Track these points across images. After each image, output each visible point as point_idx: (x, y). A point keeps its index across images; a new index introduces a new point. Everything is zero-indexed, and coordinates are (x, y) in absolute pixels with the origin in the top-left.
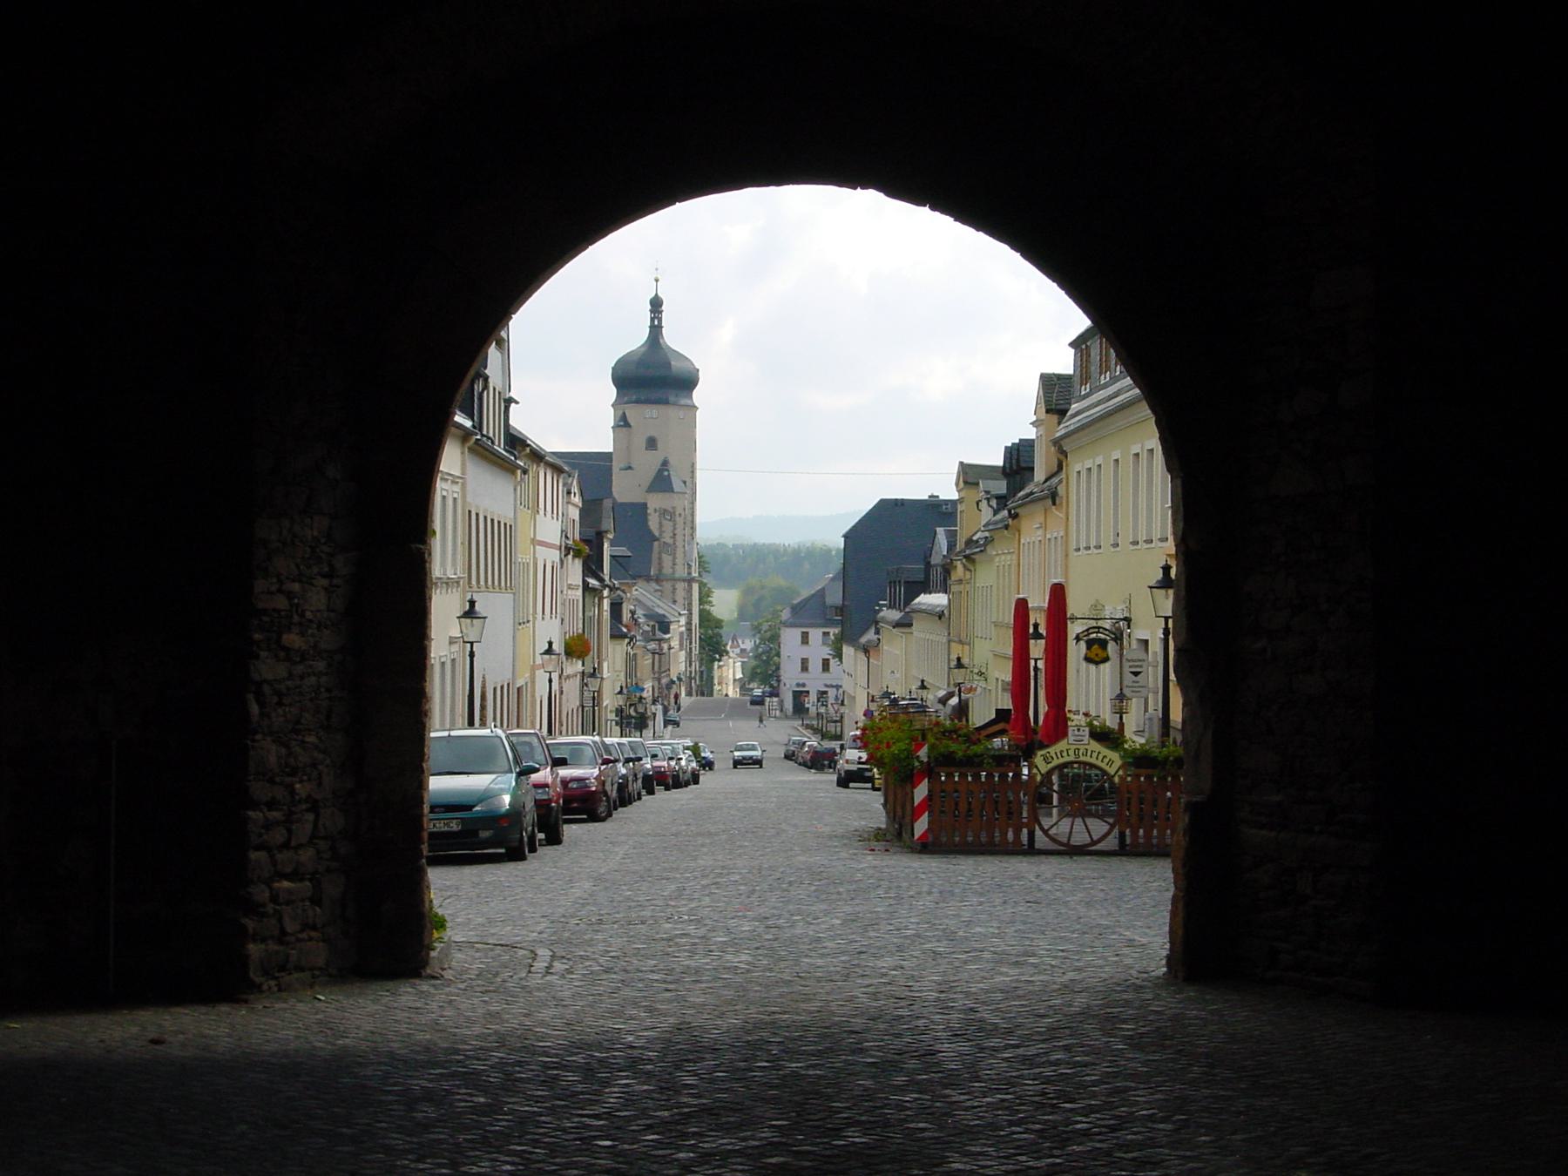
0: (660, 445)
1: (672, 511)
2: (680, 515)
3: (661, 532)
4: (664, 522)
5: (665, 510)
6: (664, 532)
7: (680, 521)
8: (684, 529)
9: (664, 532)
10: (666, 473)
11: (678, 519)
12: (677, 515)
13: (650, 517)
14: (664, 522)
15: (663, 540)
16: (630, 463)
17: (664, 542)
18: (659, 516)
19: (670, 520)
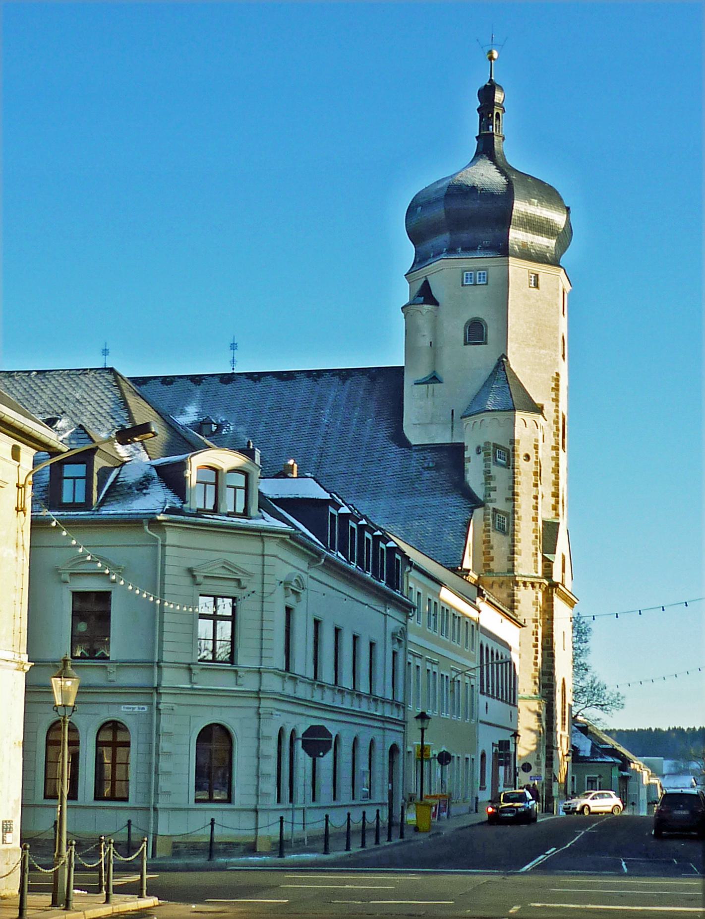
0: (491, 333)
1: (510, 447)
2: (528, 457)
3: (489, 490)
4: (495, 470)
5: (496, 446)
7: (524, 469)
11: (520, 462)
12: (522, 457)
13: (468, 466)
14: (495, 470)
15: (491, 505)
16: (434, 372)
17: (495, 511)
18: (485, 460)
19: (507, 466)
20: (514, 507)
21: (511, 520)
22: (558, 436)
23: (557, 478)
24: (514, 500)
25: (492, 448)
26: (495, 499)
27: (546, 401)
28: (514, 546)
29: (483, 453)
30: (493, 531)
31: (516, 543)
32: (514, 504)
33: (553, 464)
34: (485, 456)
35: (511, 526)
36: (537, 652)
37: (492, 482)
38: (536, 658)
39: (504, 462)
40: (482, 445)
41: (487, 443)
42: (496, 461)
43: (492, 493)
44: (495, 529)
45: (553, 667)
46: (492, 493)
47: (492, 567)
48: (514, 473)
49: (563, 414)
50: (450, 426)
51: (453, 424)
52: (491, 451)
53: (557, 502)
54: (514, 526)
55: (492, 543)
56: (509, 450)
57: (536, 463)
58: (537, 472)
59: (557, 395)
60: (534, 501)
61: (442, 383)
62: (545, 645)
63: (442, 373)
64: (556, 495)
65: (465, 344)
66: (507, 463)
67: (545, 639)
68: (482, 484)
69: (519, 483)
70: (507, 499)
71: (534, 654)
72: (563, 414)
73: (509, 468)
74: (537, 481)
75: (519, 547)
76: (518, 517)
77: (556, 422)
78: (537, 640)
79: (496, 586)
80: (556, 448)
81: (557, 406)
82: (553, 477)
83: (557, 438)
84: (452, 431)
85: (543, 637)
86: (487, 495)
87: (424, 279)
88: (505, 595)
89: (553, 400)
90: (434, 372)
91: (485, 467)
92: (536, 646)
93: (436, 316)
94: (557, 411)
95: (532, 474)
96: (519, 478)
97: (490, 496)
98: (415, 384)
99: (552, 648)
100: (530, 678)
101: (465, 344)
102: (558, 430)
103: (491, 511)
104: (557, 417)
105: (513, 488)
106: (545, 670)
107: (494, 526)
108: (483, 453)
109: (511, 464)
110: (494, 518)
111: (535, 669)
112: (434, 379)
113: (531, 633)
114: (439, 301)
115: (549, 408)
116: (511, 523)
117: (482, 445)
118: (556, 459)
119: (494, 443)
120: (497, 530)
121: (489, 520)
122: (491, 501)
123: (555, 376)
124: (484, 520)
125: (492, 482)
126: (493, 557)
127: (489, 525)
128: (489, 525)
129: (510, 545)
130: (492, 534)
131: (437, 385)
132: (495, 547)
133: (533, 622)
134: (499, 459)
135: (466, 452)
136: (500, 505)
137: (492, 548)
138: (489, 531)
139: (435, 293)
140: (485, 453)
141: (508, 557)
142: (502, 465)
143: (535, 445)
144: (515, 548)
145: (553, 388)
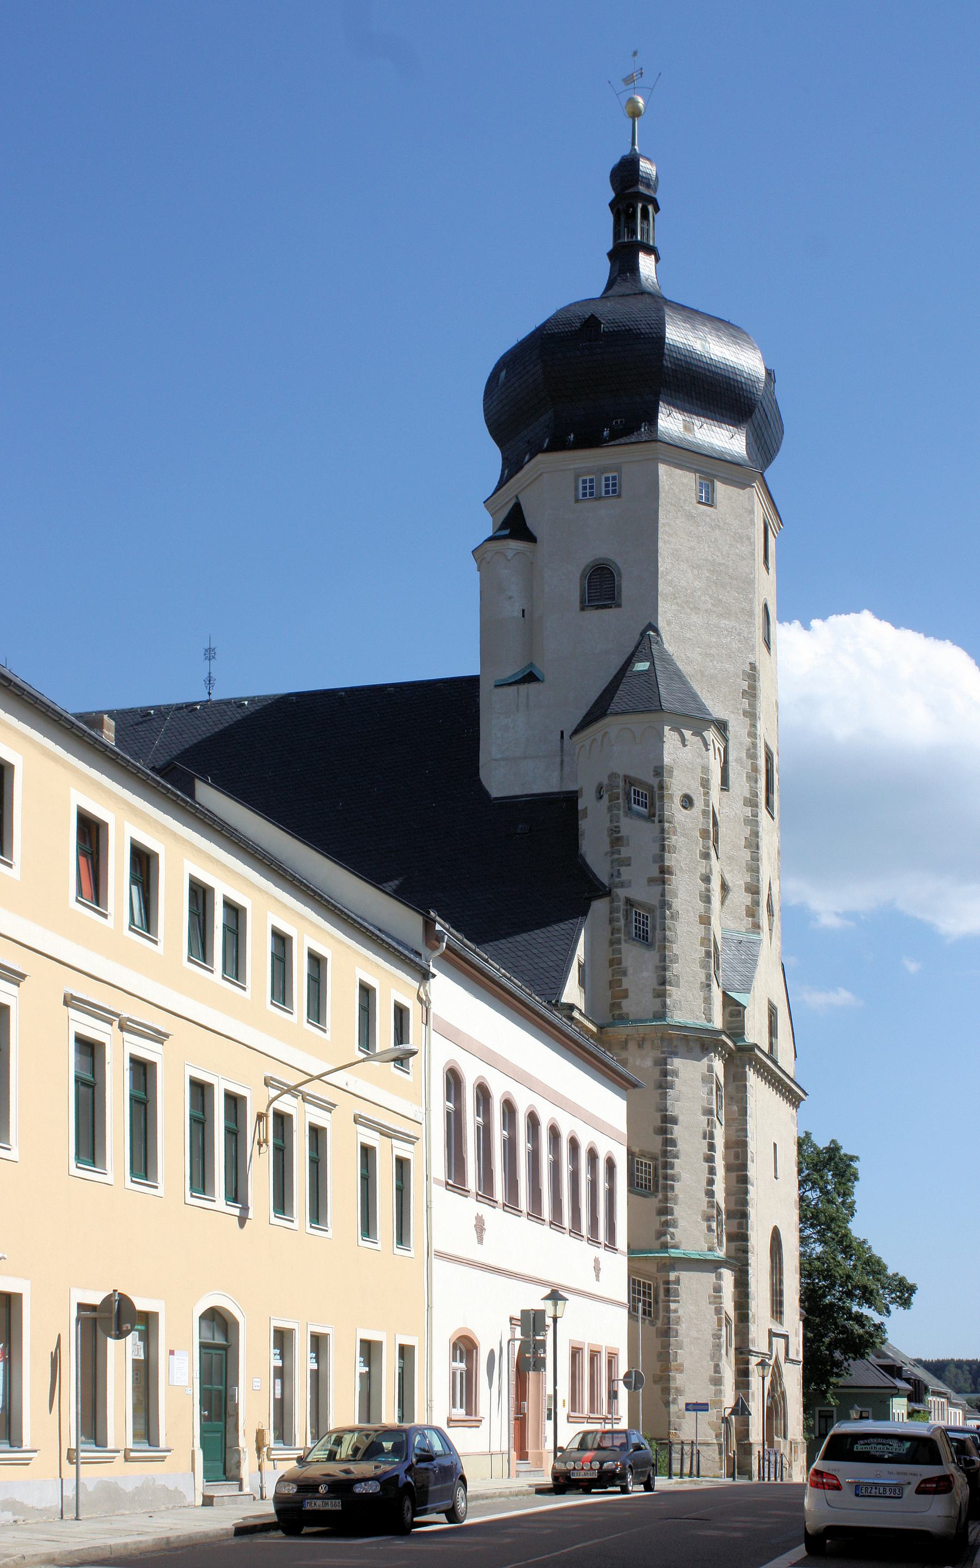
0: (628, 588)
2: (688, 802)
4: (628, 825)
5: (629, 781)
6: (627, 862)
8: (706, 856)
9: (627, 862)
10: (642, 666)
13: (583, 824)
14: (628, 825)
15: (621, 893)
16: (531, 665)
17: (629, 902)
18: (610, 809)
20: (663, 895)
21: (658, 920)
22: (756, 782)
23: (756, 858)
24: (663, 882)
25: (621, 784)
26: (630, 881)
27: (732, 716)
28: (664, 969)
29: (606, 797)
30: (625, 941)
31: (668, 964)
32: (664, 889)
33: (747, 831)
34: (610, 801)
35: (658, 932)
36: (712, 1171)
37: (623, 849)
38: (711, 1182)
39: (643, 809)
40: (605, 781)
41: (613, 776)
42: (630, 809)
43: (623, 870)
44: (630, 939)
45: (745, 1203)
46: (623, 870)
47: (625, 1010)
48: (663, 831)
49: (766, 746)
50: (558, 759)
51: (562, 755)
52: (620, 791)
53: (756, 903)
54: (664, 929)
55: (624, 965)
56: (653, 787)
57: (705, 813)
58: (708, 831)
59: (753, 705)
60: (703, 886)
61: (543, 681)
62: (732, 1160)
63: (541, 668)
64: (753, 890)
65: (582, 609)
66: (650, 812)
67: (732, 1151)
68: (606, 854)
69: (674, 849)
70: (651, 881)
71: (705, 1176)
72: (766, 746)
73: (653, 822)
74: (708, 848)
75: (676, 969)
76: (672, 913)
77: (752, 756)
78: (712, 1147)
79: (632, 1046)
80: (752, 802)
81: (754, 726)
82: (746, 855)
83: (753, 785)
84: (562, 770)
85: (727, 1146)
86: (615, 874)
87: (514, 501)
88: (649, 1063)
89: (745, 713)
90: (531, 665)
91: (611, 821)
92: (710, 1159)
93: (532, 563)
94: (753, 735)
95: (698, 834)
96: (674, 840)
97: (619, 874)
98: (496, 686)
99: (744, 1167)
100: (699, 1219)
101: (582, 609)
102: (755, 769)
103: (621, 904)
104: (754, 745)
105: (662, 858)
106: (733, 1207)
107: (628, 933)
108: (606, 797)
109: (657, 813)
110: (627, 916)
111: (709, 1202)
112: (530, 677)
113: (701, 1135)
114: (536, 534)
115: (738, 728)
116: (658, 926)
117: (605, 781)
118: (753, 822)
119: (625, 776)
120: (634, 940)
121: (618, 920)
122: (622, 885)
123: (747, 668)
124: (611, 921)
125: (623, 849)
126: (626, 990)
127: (619, 930)
128: (619, 930)
129: (657, 967)
130: (624, 946)
131: (533, 687)
132: (630, 971)
133: (704, 1114)
134: (635, 806)
135: (580, 801)
136: (640, 892)
137: (624, 973)
138: (619, 942)
139: (531, 522)
140: (609, 795)
141: (654, 990)
142: (639, 815)
143: (702, 779)
144: (667, 973)
145: (744, 691)
